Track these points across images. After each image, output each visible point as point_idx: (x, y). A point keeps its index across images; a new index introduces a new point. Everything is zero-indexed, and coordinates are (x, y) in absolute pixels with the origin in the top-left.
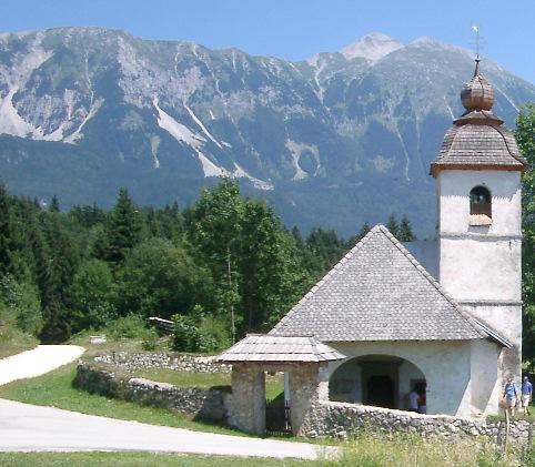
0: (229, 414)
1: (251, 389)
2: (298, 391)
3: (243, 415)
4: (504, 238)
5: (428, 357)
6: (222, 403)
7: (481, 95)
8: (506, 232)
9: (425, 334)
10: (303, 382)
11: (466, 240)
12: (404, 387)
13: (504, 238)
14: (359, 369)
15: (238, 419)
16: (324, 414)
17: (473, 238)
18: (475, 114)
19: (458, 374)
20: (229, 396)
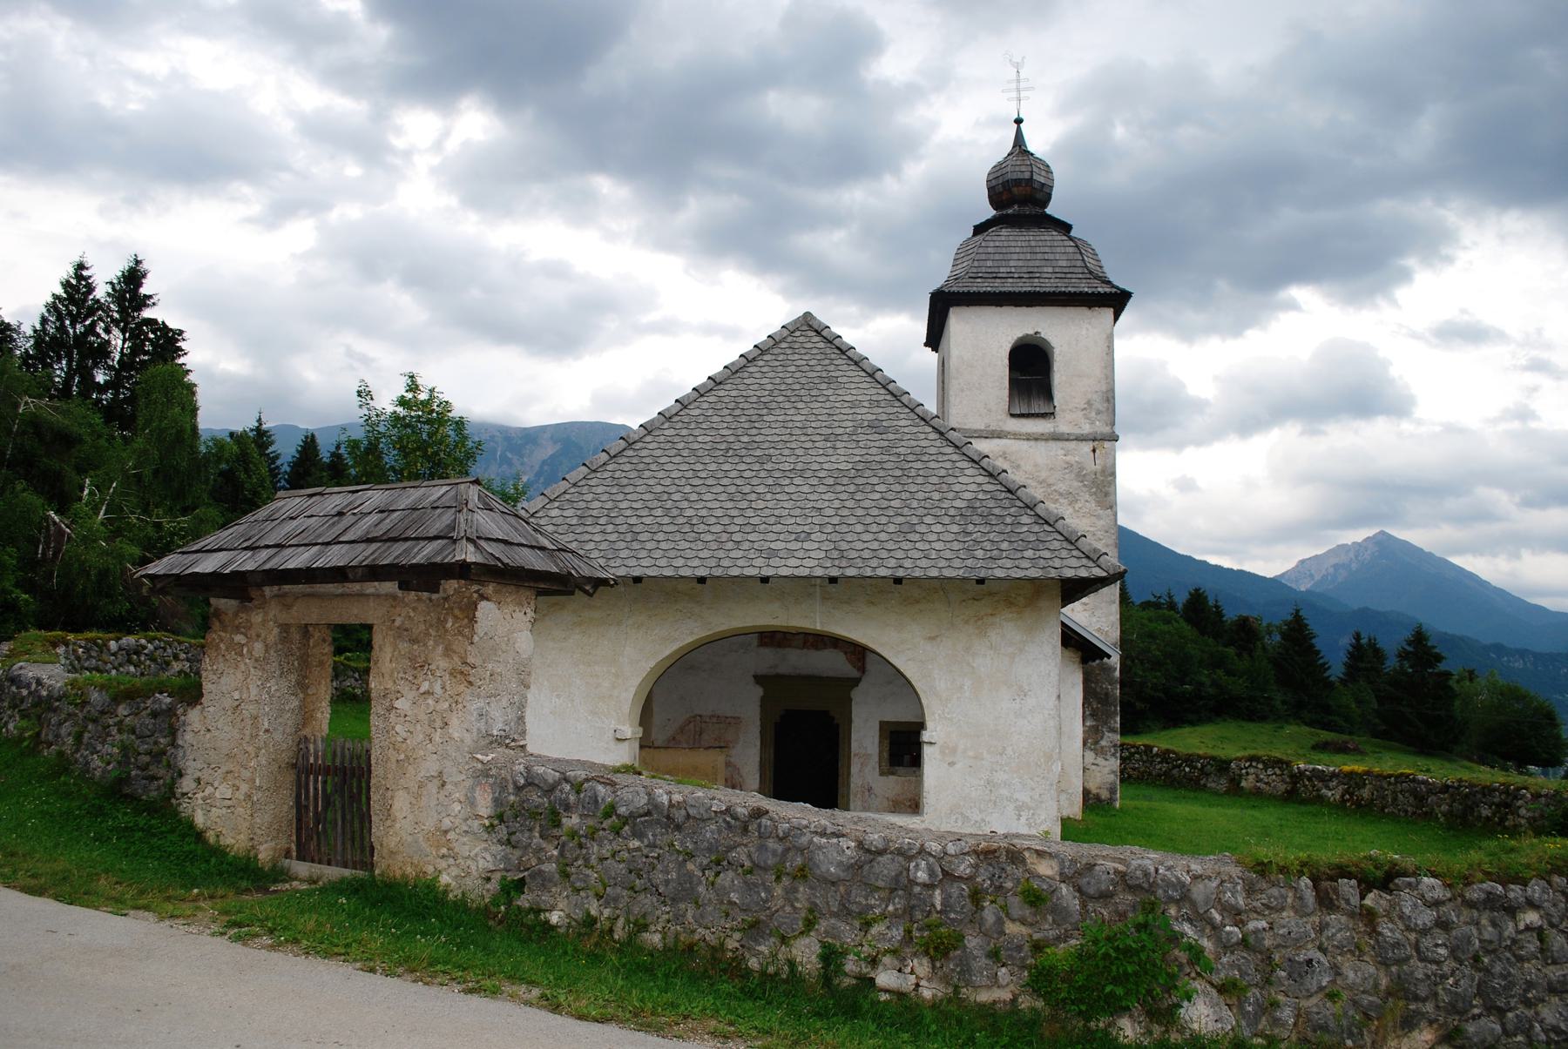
0: (187, 784)
3: (224, 791)
4: (1081, 439)
5: (932, 639)
6: (173, 732)
7: (1027, 175)
8: (1086, 429)
9: (924, 563)
11: (1004, 441)
12: (865, 742)
13: (1081, 439)
14: (759, 691)
15: (208, 803)
16: (485, 807)
17: (1016, 436)
19: (1023, 693)
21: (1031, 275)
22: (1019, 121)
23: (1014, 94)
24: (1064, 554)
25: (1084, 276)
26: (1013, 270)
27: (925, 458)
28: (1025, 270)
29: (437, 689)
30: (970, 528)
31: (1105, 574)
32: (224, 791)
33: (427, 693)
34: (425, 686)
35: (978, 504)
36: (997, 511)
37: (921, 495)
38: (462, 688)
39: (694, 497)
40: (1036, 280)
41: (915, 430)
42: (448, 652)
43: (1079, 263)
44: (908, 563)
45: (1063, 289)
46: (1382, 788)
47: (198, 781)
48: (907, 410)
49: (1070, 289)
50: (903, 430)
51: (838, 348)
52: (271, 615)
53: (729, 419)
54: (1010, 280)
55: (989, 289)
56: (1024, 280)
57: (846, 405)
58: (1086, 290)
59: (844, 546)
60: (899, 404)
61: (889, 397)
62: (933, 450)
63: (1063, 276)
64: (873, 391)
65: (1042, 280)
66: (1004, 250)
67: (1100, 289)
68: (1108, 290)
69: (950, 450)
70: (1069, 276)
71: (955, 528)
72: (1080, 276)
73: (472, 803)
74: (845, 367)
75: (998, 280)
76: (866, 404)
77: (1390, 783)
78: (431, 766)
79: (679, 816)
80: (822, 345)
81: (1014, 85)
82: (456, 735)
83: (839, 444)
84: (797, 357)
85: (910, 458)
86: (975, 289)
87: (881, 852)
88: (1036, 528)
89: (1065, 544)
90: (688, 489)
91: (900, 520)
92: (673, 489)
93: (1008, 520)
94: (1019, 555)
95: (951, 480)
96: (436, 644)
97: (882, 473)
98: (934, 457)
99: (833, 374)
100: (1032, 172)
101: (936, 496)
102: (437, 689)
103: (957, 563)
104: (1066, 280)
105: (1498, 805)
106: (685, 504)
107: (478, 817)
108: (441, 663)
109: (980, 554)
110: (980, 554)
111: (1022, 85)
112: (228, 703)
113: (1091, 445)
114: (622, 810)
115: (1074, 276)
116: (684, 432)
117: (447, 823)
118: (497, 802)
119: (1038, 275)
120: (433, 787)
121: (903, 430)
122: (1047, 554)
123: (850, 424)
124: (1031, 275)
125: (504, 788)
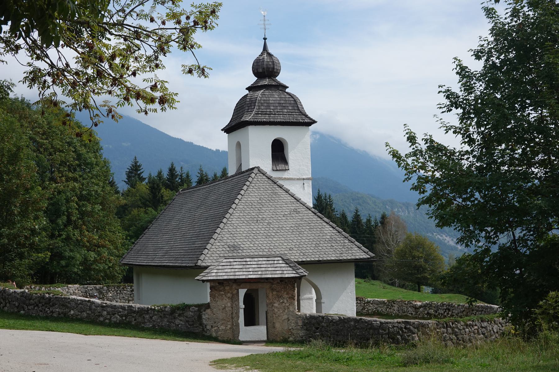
1: (229, 305)
2: (276, 305)
3: (223, 327)
7: (272, 66)
9: (325, 256)
10: (280, 297)
15: (216, 331)
16: (300, 323)
18: (266, 82)
20: (208, 311)
21: (279, 113)
22: (265, 39)
23: (263, 26)
24: (358, 251)
25: (299, 114)
26: (272, 111)
27: (314, 222)
28: (276, 111)
29: (285, 301)
30: (333, 245)
31: (369, 257)
32: (223, 327)
33: (283, 302)
34: (282, 301)
35: (332, 237)
36: (338, 239)
37: (317, 235)
38: (292, 301)
39: (256, 237)
40: (281, 116)
41: (307, 212)
42: (287, 294)
43: (296, 108)
44: (321, 256)
45: (292, 120)
46: (402, 306)
47: (212, 327)
48: (302, 205)
49: (295, 120)
50: (304, 212)
51: (272, 181)
52: (234, 287)
53: (252, 209)
54: (272, 115)
55: (265, 120)
56: (277, 115)
57: (284, 203)
58: (301, 120)
59: (304, 252)
60: (299, 203)
61: (295, 200)
62: (315, 219)
63: (290, 113)
64: (290, 198)
65: (283, 116)
66: (268, 102)
67: (306, 120)
68: (309, 121)
69: (319, 219)
70: (293, 114)
71: (330, 245)
72: (297, 114)
73: (297, 323)
74: (277, 189)
75: (267, 116)
76: (289, 203)
77: (405, 304)
78: (285, 317)
79: (346, 321)
80: (267, 179)
81: (263, 22)
82: (291, 310)
83: (288, 218)
84: (262, 185)
85: (310, 222)
86: (260, 120)
87: (384, 323)
88: (349, 244)
89: (358, 249)
90: (253, 235)
91: (314, 243)
92: (248, 235)
93: (342, 242)
94: (347, 252)
95: (323, 229)
96: (284, 292)
97: (304, 228)
98: (316, 222)
99: (275, 191)
100: (274, 64)
101: (321, 235)
102: (285, 301)
103: (334, 255)
104: (292, 116)
105: (445, 309)
106: (254, 240)
107: (299, 326)
108: (285, 296)
109: (338, 252)
110: (338, 252)
111: (266, 22)
112: (221, 308)
113: (302, 182)
114: (334, 321)
115: (295, 114)
116: (241, 214)
117: (291, 328)
118: (303, 322)
119: (281, 113)
120: (286, 321)
121: (304, 212)
122: (355, 252)
123: (288, 211)
124: (279, 113)
125: (304, 319)
